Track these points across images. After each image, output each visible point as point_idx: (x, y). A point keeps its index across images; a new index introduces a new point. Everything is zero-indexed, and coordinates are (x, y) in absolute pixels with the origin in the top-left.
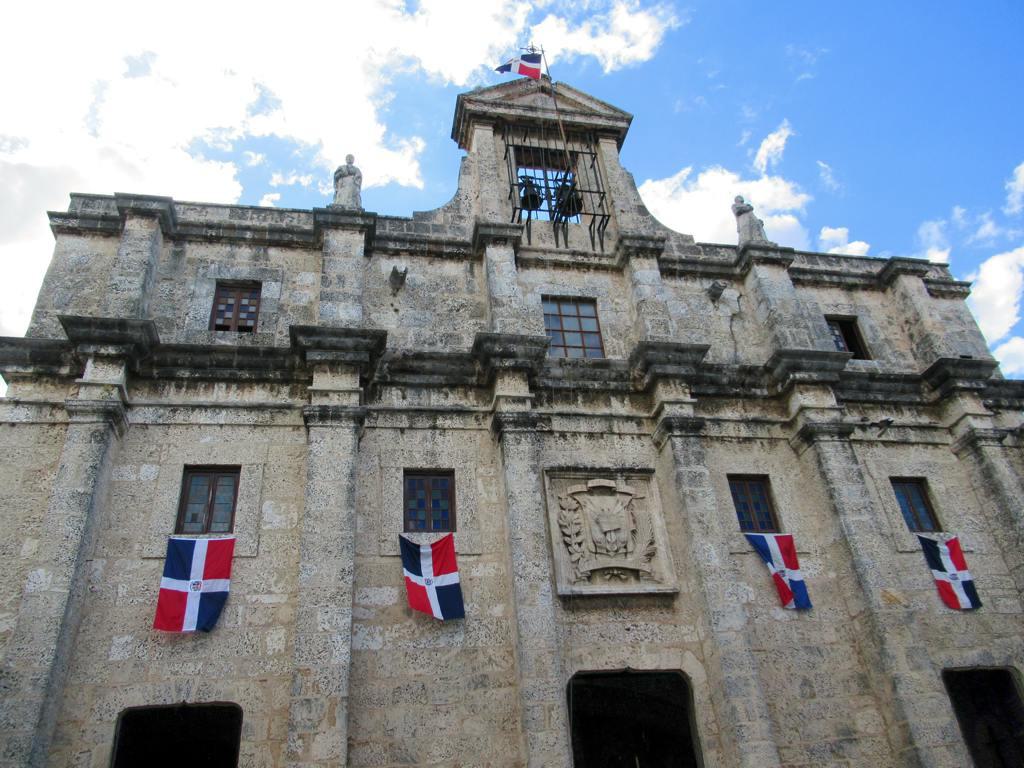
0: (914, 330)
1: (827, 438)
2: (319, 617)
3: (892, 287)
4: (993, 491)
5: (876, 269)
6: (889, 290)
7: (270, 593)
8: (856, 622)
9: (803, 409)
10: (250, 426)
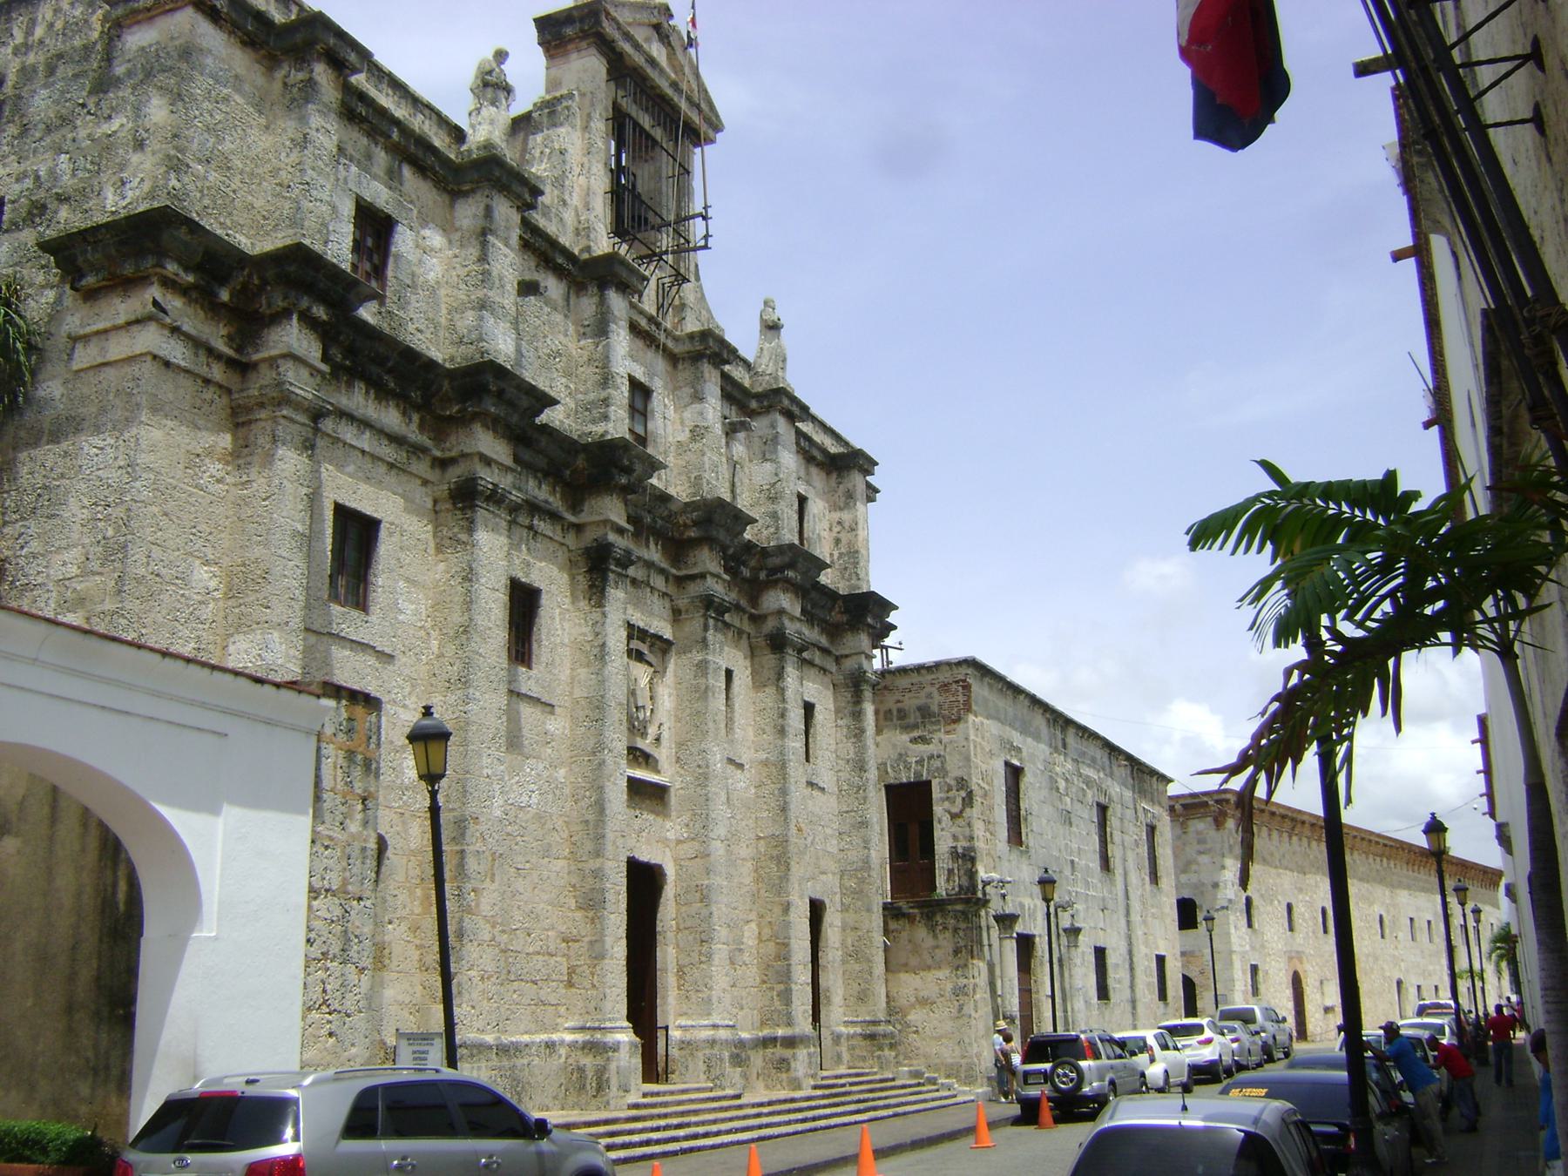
0: (844, 537)
1: (790, 651)
2: (485, 761)
3: (839, 476)
4: (855, 736)
5: (834, 448)
6: (834, 476)
7: (405, 706)
8: (762, 842)
9: (781, 612)
10: (388, 463)
